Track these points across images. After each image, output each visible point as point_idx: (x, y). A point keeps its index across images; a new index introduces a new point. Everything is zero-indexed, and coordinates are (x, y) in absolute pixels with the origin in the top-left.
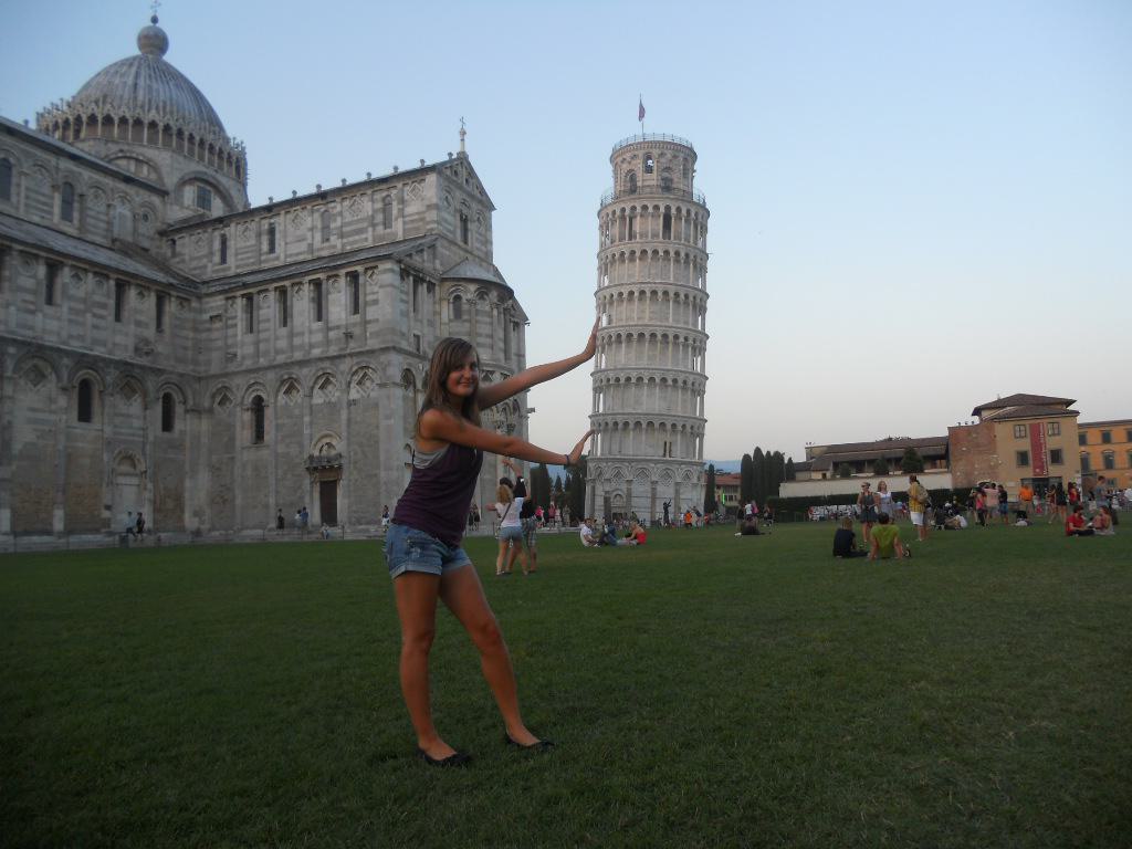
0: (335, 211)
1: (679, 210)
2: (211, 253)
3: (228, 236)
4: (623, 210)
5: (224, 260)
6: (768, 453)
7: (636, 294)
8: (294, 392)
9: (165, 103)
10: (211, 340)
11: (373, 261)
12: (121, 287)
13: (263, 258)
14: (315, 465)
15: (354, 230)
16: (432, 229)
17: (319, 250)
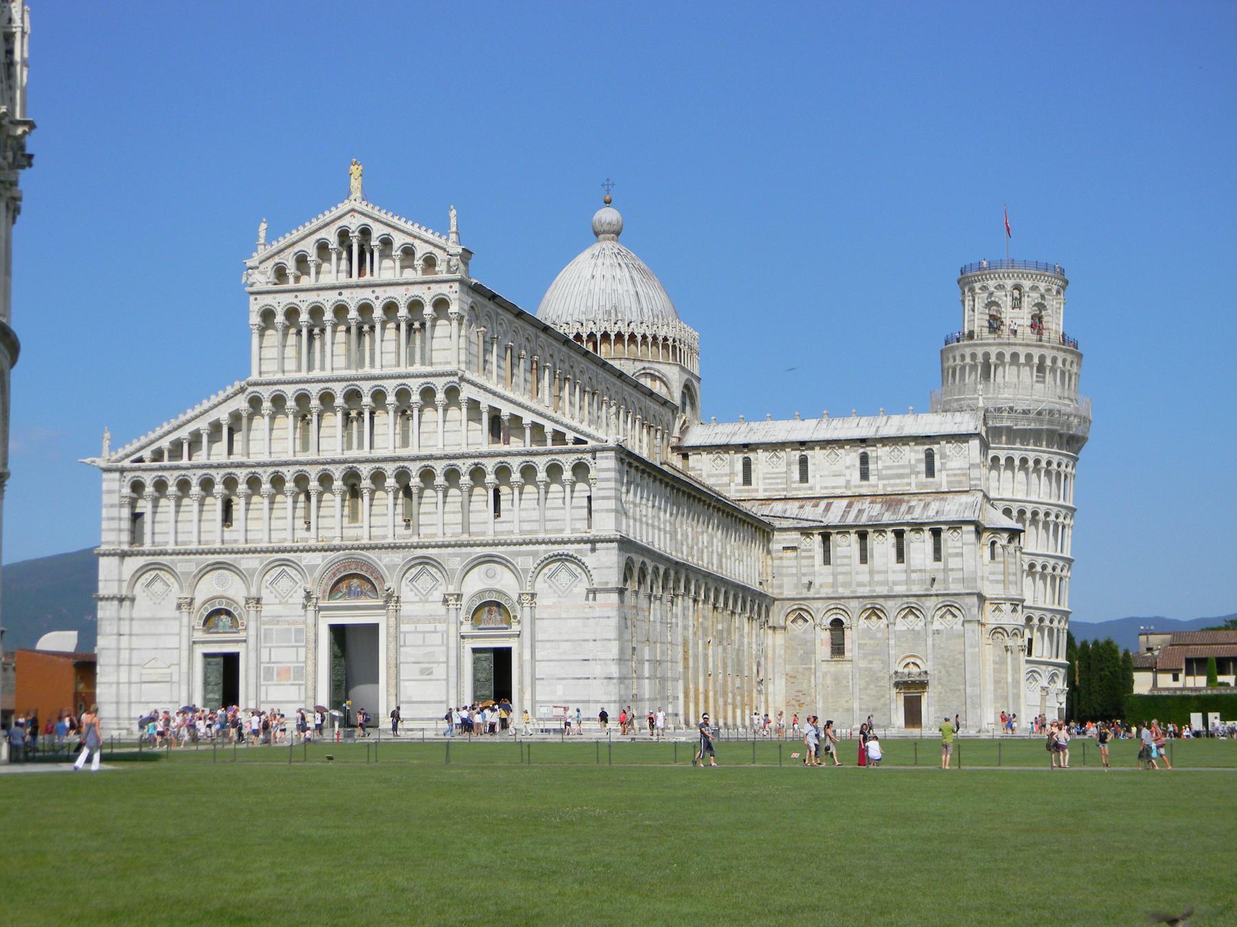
0: (874, 454)
1: (1054, 360)
2: (732, 474)
3: (752, 460)
4: (987, 356)
5: (747, 480)
6: (1096, 643)
7: (1002, 462)
8: (874, 618)
9: (662, 312)
10: (788, 567)
11: (956, 525)
12: (756, 527)
13: (794, 486)
14: (898, 679)
15: (896, 474)
16: (975, 485)
17: (856, 486)
